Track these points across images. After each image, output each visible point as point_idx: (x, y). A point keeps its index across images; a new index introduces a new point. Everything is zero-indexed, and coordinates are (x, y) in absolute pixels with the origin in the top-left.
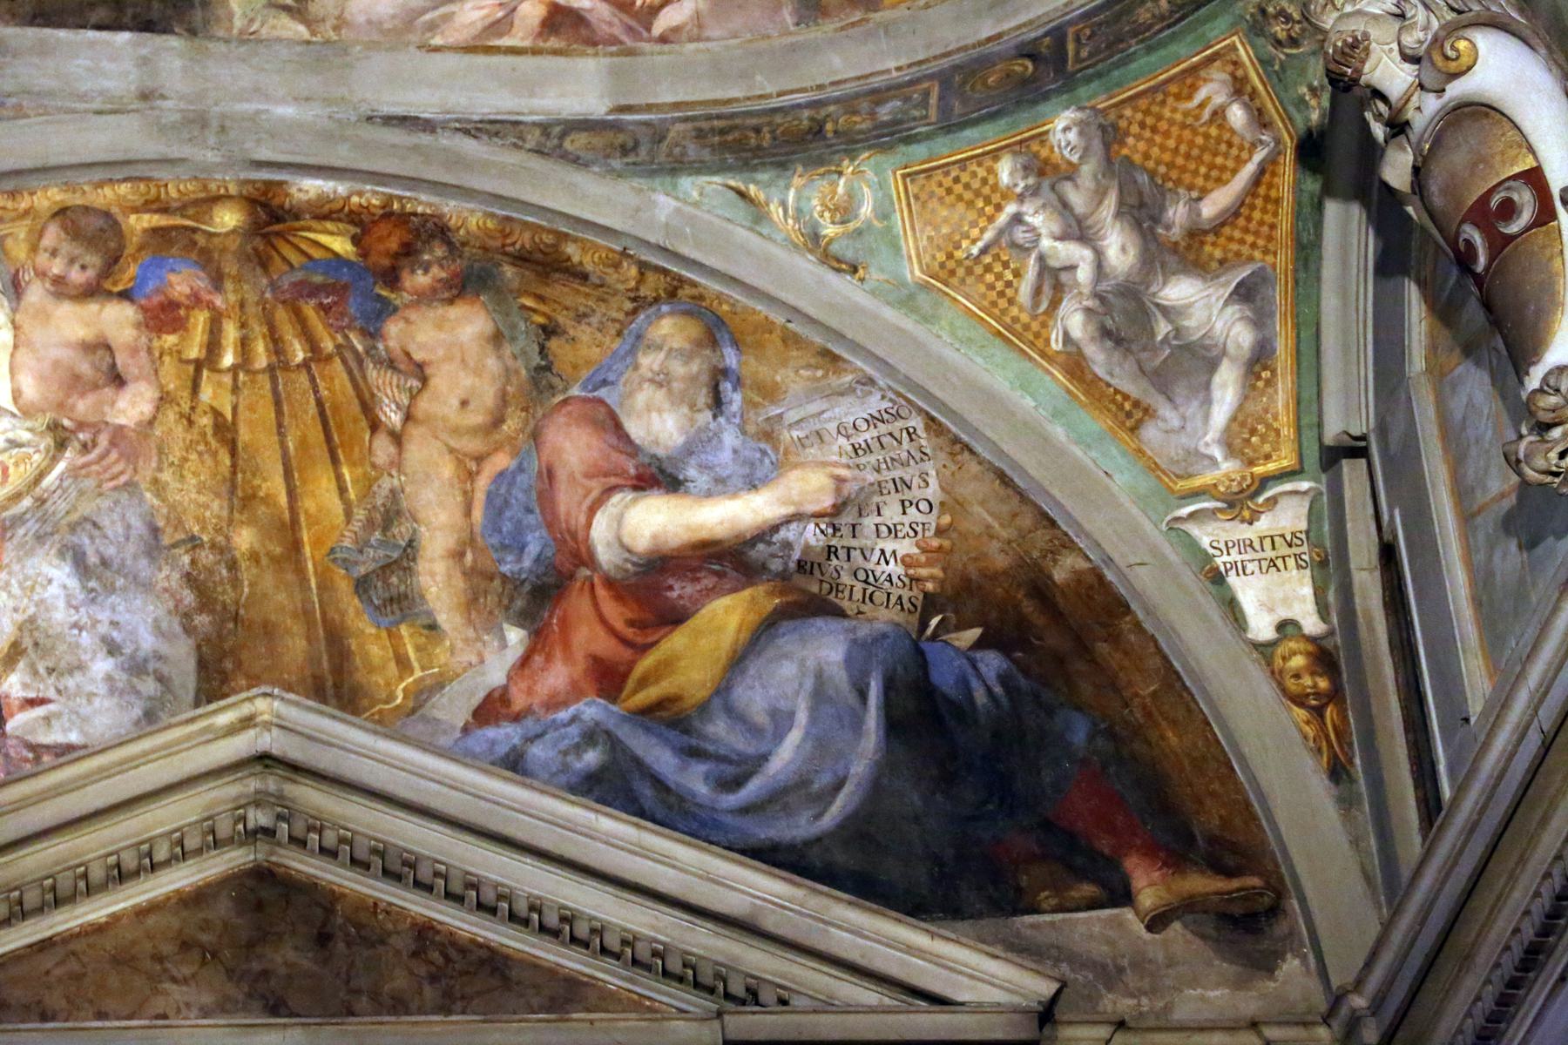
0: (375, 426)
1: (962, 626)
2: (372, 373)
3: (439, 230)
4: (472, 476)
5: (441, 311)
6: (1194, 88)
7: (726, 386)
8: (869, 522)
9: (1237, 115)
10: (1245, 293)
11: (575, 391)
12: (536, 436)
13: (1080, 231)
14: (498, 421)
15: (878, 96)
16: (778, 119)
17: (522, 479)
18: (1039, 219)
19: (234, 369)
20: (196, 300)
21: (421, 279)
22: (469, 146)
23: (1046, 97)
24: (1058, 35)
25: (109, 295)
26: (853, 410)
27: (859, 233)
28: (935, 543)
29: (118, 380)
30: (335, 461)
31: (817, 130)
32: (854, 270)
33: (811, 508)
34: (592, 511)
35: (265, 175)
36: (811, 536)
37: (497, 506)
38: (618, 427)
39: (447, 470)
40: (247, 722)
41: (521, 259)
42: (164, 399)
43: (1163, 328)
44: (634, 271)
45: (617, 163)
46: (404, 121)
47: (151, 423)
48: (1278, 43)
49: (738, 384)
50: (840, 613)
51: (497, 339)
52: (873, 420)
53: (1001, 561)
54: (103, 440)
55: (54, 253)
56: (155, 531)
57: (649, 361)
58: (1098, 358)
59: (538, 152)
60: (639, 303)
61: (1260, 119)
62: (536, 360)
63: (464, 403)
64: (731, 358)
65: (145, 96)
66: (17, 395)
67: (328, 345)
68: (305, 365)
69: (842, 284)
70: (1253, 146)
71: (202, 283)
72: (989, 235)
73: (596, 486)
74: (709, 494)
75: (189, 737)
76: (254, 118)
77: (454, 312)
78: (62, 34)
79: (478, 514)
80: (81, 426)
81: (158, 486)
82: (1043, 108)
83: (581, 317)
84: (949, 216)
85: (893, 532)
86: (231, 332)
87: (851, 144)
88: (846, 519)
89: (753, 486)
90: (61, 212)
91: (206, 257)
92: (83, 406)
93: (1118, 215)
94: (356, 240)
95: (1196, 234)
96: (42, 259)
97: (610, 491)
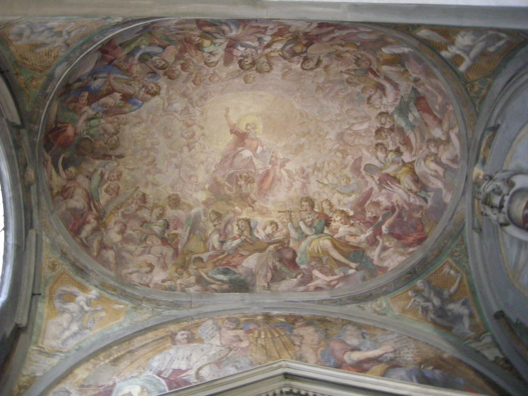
0: (295, 345)
1: (428, 366)
2: (292, 337)
3: (302, 317)
4: (316, 351)
5: (304, 328)
6: (443, 270)
7: (365, 335)
8: (402, 352)
9: (452, 272)
10: (464, 304)
11: (334, 338)
12: (328, 345)
13: (428, 300)
14: (319, 343)
15: (381, 287)
16: (363, 295)
17: (327, 351)
18: (419, 300)
19: (264, 338)
20: (255, 329)
21: (299, 324)
22: (304, 303)
23: (414, 279)
24: (414, 268)
25: (239, 329)
26: (391, 337)
27: (384, 309)
28: (417, 354)
29: (241, 341)
30: (286, 349)
31: (371, 295)
32: (385, 315)
33: (389, 351)
34: (344, 354)
35: (266, 311)
36: (391, 355)
37: (323, 355)
38: (345, 342)
39: (311, 351)
40: (280, 367)
41: (318, 320)
42: (251, 343)
43: (450, 314)
44: (341, 320)
45: (334, 304)
46: (291, 301)
47: (249, 346)
48: (456, 256)
49: (367, 334)
50: (400, 367)
51: (316, 331)
52: (397, 337)
53: (432, 356)
54: (239, 349)
55: (227, 324)
56: (252, 362)
57: (348, 333)
58: (439, 320)
59: (318, 304)
60: (344, 325)
61: (457, 272)
62: (325, 334)
63: (312, 341)
64: (364, 331)
65: (242, 300)
66: (221, 343)
67: (282, 334)
68: (279, 337)
69: (384, 317)
70: (457, 277)
71: (256, 326)
72: (410, 304)
73: (343, 351)
74: (367, 351)
75: (267, 369)
76: (263, 302)
77: (307, 328)
78: (227, 294)
79: (319, 357)
80: (235, 347)
81: (251, 356)
82: (415, 281)
83: (332, 327)
84: (402, 303)
85: (407, 353)
86: (263, 333)
87: (378, 296)
88: (397, 352)
89: (375, 348)
90: (228, 318)
91: (257, 323)
92: (235, 345)
93: (435, 295)
94: (285, 319)
95: (451, 296)
96: (225, 325)
97: (347, 351)
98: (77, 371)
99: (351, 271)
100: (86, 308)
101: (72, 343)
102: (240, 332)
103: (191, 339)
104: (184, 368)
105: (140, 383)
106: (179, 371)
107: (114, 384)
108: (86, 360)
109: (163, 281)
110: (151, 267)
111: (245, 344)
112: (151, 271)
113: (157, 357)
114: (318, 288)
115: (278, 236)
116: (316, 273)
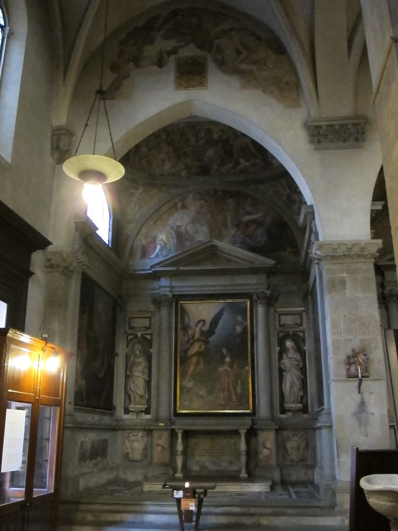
98: (143, 229)
99: (258, 161)
100: (140, 197)
101: (138, 216)
102: (203, 202)
103: (184, 207)
104: (180, 225)
105: (165, 233)
106: (179, 227)
107: (156, 234)
108: (145, 223)
109: (170, 169)
110: (164, 161)
111: (204, 210)
112: (164, 164)
113: (171, 219)
114: (241, 172)
115: (225, 137)
116: (242, 160)
